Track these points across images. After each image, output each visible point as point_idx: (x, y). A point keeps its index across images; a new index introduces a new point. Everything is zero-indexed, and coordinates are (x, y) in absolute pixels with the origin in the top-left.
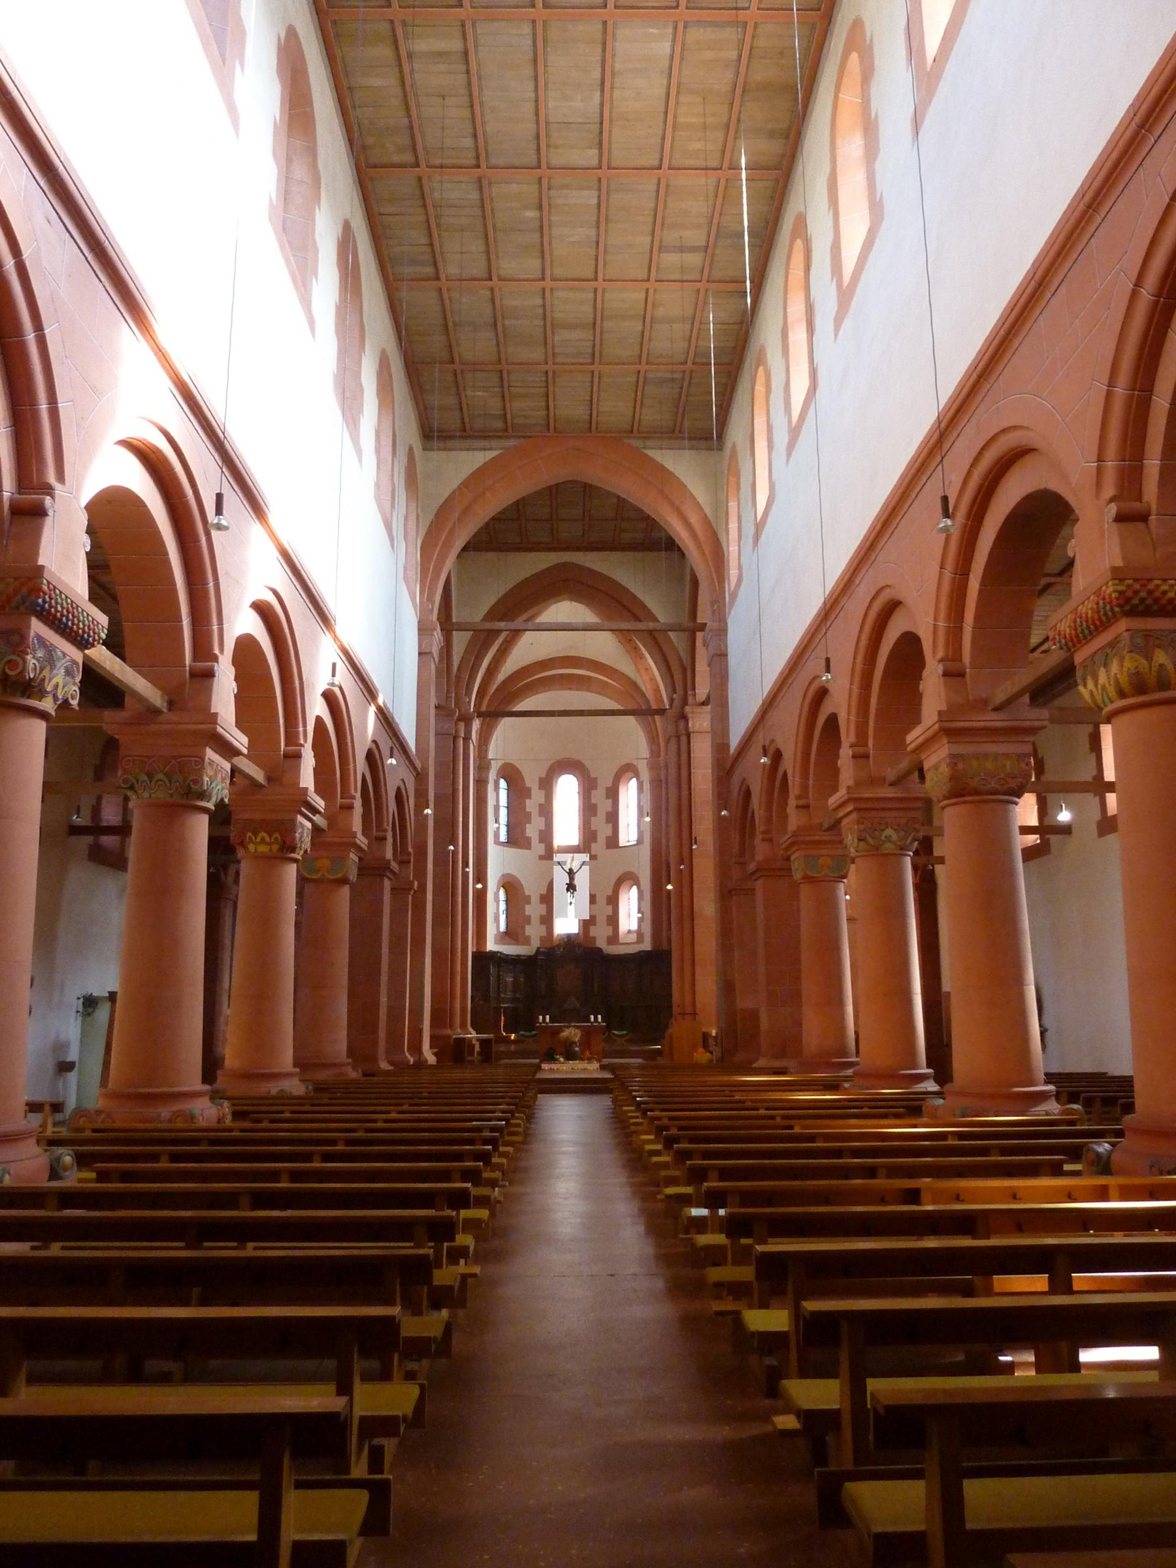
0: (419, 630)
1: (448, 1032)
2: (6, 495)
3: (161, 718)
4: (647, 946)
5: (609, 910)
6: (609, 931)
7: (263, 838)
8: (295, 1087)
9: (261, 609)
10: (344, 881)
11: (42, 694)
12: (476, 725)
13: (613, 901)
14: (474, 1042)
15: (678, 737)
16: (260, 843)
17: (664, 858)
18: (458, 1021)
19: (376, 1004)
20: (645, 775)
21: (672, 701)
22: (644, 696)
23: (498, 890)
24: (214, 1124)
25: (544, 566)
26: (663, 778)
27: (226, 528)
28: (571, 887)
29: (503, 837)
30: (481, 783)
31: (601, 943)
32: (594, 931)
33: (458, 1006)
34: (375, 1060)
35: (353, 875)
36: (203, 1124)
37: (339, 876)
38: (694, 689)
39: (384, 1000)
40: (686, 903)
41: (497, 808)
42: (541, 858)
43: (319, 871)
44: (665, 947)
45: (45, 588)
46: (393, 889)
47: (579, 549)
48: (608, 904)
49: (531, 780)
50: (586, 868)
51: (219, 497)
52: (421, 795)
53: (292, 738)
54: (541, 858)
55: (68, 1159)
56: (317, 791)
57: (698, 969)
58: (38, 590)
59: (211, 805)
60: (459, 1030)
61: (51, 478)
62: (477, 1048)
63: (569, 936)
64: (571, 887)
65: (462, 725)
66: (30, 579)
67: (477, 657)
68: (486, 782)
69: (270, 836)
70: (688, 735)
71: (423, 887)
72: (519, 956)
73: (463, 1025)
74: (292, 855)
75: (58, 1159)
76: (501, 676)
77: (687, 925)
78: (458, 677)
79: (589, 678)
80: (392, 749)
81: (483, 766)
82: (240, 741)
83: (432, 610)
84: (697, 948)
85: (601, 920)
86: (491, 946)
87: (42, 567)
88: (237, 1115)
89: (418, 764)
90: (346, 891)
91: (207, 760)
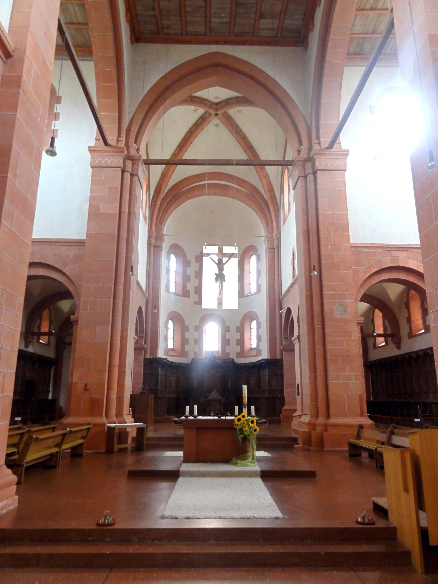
1: (104, 420)
4: (265, 355)
5: (238, 336)
6: (238, 349)
13: (241, 330)
14: (128, 430)
15: (305, 177)
17: (277, 297)
18: (113, 411)
20: (263, 248)
21: (299, 152)
22: (262, 197)
23: (168, 321)
25: (199, 54)
26: (275, 245)
28: (220, 277)
29: (172, 289)
31: (233, 356)
32: (228, 349)
33: (114, 396)
38: (318, 138)
40: (317, 308)
41: (168, 270)
42: (196, 303)
44: (278, 357)
47: (226, 43)
48: (237, 332)
49: (191, 257)
50: (234, 261)
54: (196, 303)
57: (330, 365)
60: (115, 419)
62: (133, 433)
63: (213, 352)
64: (220, 277)
65: (129, 164)
70: (315, 173)
73: (119, 414)
76: (172, 182)
77: (318, 326)
78: (128, 131)
79: (228, 186)
84: (328, 346)
85: (233, 342)
86: (161, 354)
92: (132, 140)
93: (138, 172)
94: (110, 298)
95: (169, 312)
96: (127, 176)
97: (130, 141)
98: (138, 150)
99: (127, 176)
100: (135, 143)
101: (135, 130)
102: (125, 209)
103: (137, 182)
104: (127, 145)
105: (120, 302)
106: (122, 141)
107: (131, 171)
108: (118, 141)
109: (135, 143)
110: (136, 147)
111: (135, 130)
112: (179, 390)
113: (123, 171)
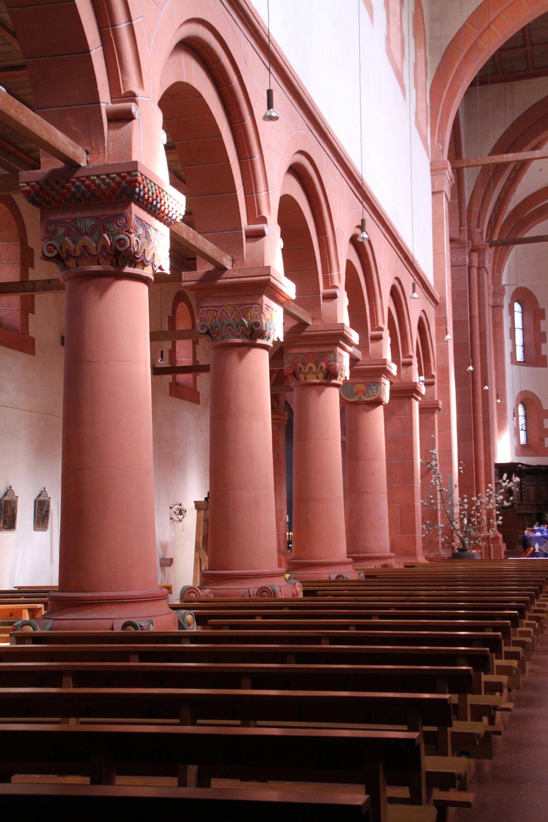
0: (432, 170)
2: (103, 106)
3: (225, 275)
7: (310, 368)
8: (351, 573)
9: (296, 171)
10: (378, 402)
11: (144, 264)
12: (489, 253)
16: (308, 373)
19: (412, 508)
24: (290, 597)
27: (276, 118)
29: (520, 357)
30: (497, 307)
34: (413, 554)
35: (386, 398)
36: (280, 596)
37: (372, 398)
39: (418, 503)
43: (356, 394)
45: (140, 179)
46: (421, 409)
51: (270, 93)
52: (441, 321)
53: (328, 280)
55: (189, 618)
56: (352, 326)
58: (134, 183)
59: (270, 343)
61: (134, 87)
65: (475, 256)
66: (129, 173)
67: (486, 193)
68: (501, 306)
69: (317, 366)
71: (448, 405)
72: (539, 466)
74: (334, 381)
75: (184, 617)
76: (511, 206)
78: (470, 211)
80: (414, 284)
81: (498, 292)
82: (289, 288)
83: (442, 151)
87: (136, 163)
88: (306, 593)
89: (437, 296)
90: (380, 410)
91: (264, 306)
92: (474, 224)
93: (484, 264)
94: (471, 414)
95: (517, 392)
96: (475, 271)
97: (472, 224)
98: (482, 233)
99: (475, 271)
100: (478, 227)
101: (476, 209)
102: (476, 313)
103: (485, 274)
104: (470, 237)
105: (480, 416)
106: (464, 230)
107: (477, 265)
108: (460, 231)
109: (478, 226)
110: (480, 231)
111: (476, 209)
112: (540, 503)
113: (470, 268)
